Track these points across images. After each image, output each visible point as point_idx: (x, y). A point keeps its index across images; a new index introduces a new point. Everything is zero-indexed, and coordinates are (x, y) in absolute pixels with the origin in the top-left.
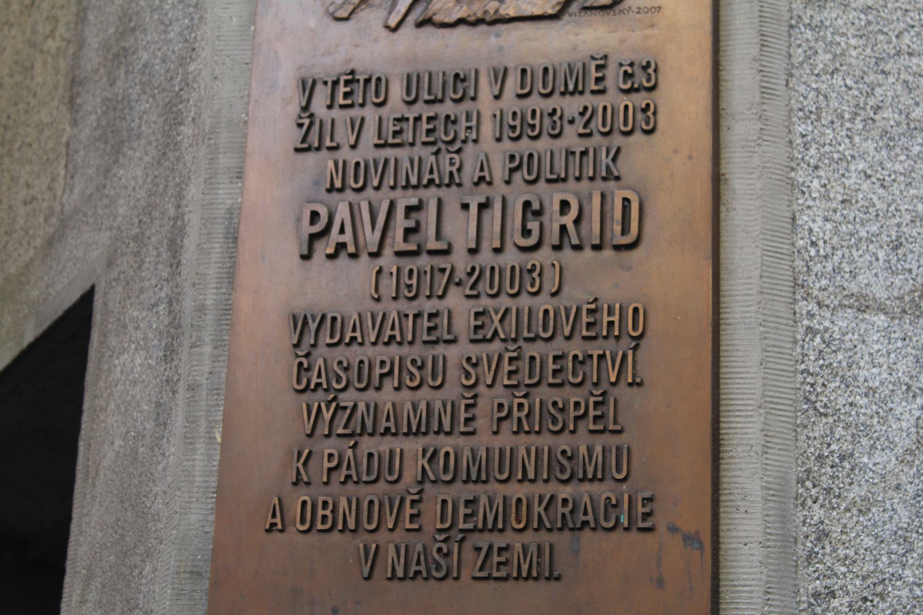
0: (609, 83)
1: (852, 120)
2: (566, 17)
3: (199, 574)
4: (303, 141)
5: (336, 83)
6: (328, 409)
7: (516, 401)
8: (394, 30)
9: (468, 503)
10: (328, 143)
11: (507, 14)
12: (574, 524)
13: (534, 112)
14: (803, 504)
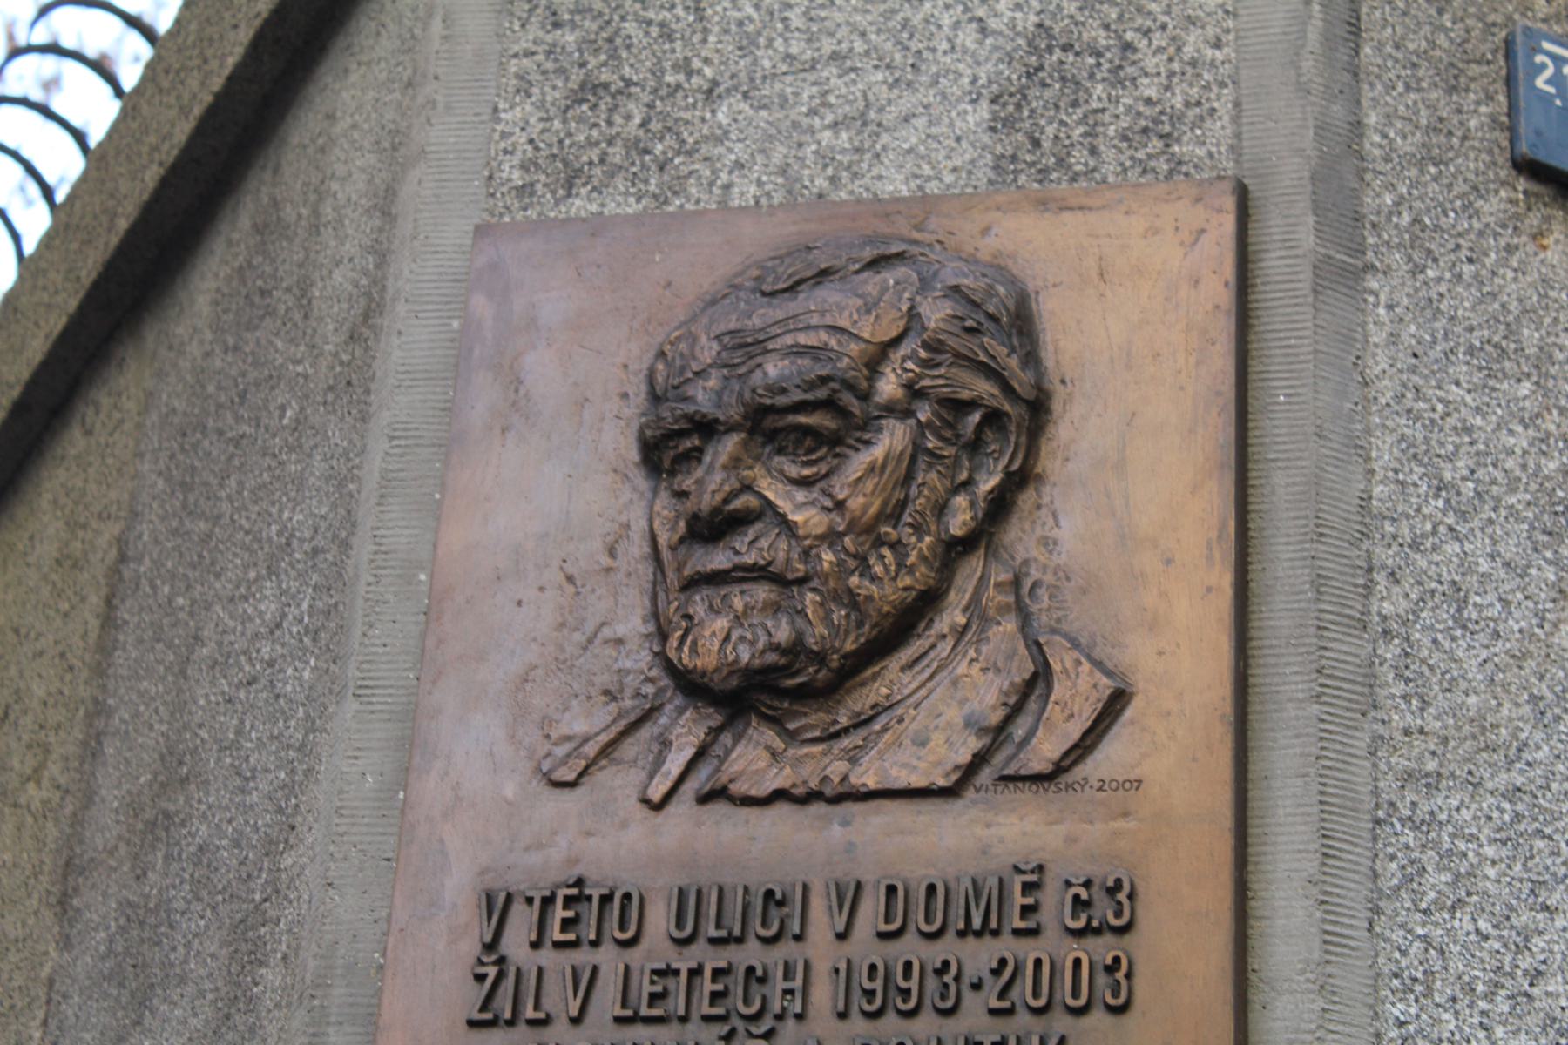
0: (1046, 916)
1: (1490, 996)
2: (970, 794)
4: (484, 1008)
5: (548, 901)
8: (658, 807)
10: (530, 1013)
11: (864, 785)
13: (908, 966)
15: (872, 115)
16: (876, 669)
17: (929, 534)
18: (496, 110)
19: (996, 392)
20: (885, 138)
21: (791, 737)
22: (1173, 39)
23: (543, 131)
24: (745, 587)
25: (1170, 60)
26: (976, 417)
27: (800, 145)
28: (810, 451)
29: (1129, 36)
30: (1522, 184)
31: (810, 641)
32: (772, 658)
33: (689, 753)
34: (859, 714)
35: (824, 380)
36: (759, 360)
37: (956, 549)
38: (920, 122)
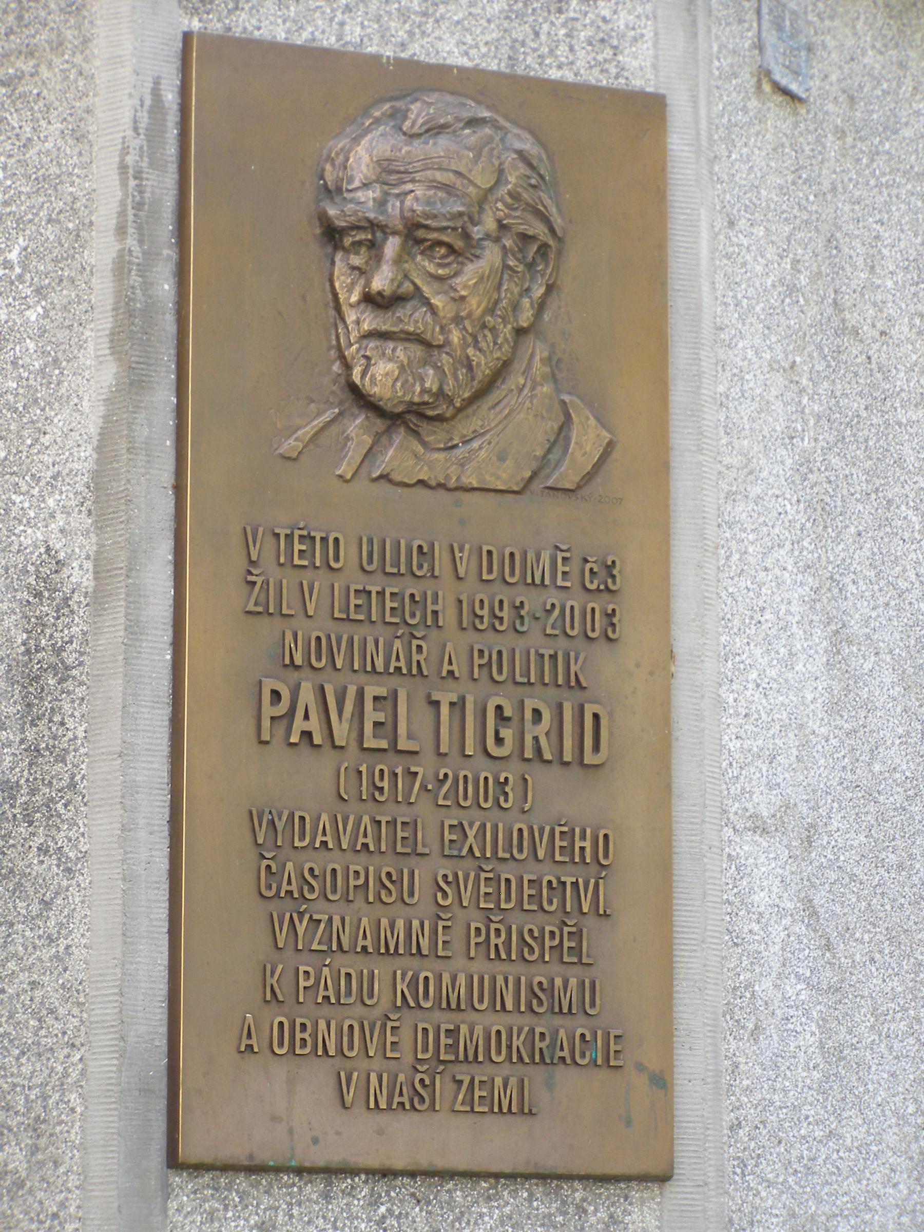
12: (552, 1059)
16: (475, 407)
17: (509, 323)
19: (547, 231)
24: (408, 345)
28: (443, 257)
32: (426, 398)
34: (465, 436)
35: (461, 214)
36: (409, 186)
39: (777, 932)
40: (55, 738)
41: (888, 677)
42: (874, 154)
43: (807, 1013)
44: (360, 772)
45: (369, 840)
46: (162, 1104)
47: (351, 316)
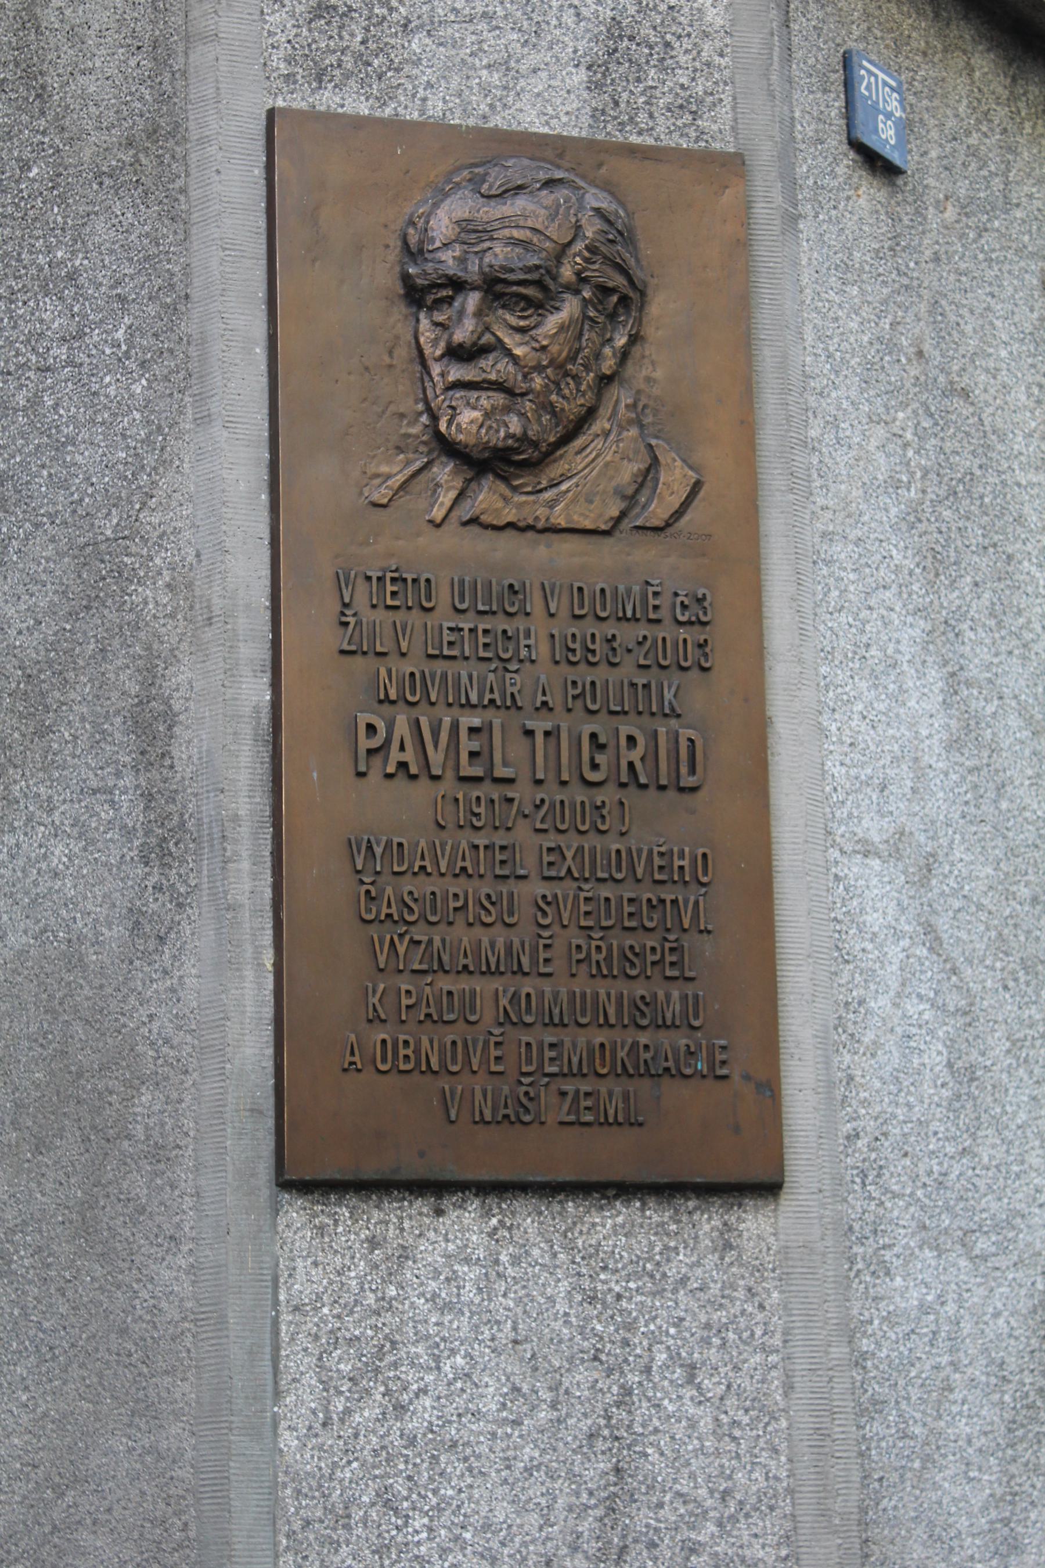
1: (852, 660)
3: (261, 1112)
6: (401, 943)
7: (594, 943)
8: (439, 526)
9: (552, 1046)
14: (837, 1051)
15: (513, 64)
18: (262, 12)
19: (625, 283)
20: (522, 83)
21: (515, 489)
22: (695, 44)
23: (296, 35)
24: (490, 394)
25: (694, 59)
26: (615, 298)
27: (468, 77)
28: (523, 310)
29: (668, 37)
30: (852, 155)
31: (530, 433)
33: (452, 494)
35: (537, 267)
36: (487, 244)
37: (605, 381)
38: (544, 75)
39: (895, 952)
40: (165, 781)
41: (1014, 721)
42: (983, 230)
43: (931, 1032)
44: (457, 800)
45: (468, 864)
46: (271, 1123)
47: (436, 369)
